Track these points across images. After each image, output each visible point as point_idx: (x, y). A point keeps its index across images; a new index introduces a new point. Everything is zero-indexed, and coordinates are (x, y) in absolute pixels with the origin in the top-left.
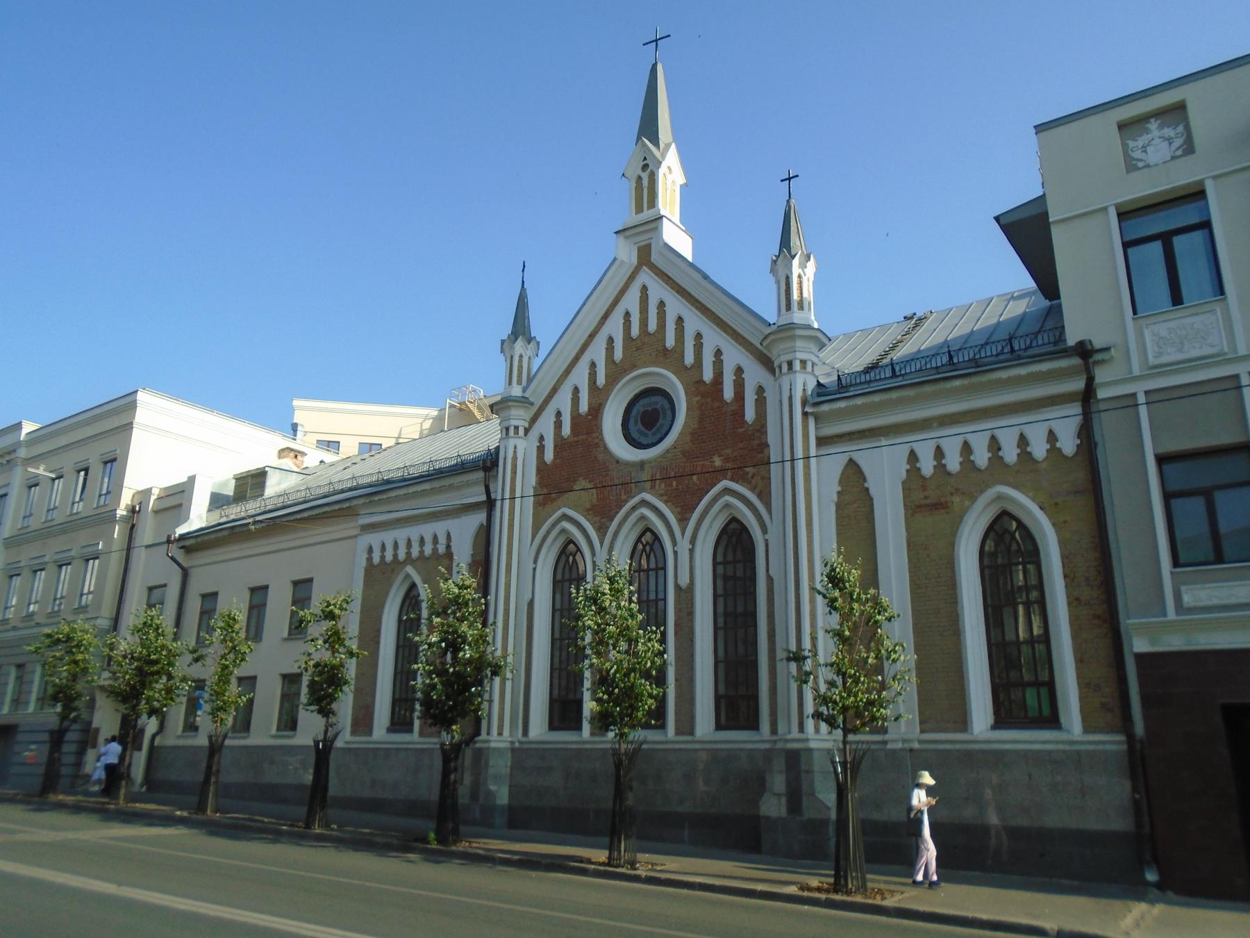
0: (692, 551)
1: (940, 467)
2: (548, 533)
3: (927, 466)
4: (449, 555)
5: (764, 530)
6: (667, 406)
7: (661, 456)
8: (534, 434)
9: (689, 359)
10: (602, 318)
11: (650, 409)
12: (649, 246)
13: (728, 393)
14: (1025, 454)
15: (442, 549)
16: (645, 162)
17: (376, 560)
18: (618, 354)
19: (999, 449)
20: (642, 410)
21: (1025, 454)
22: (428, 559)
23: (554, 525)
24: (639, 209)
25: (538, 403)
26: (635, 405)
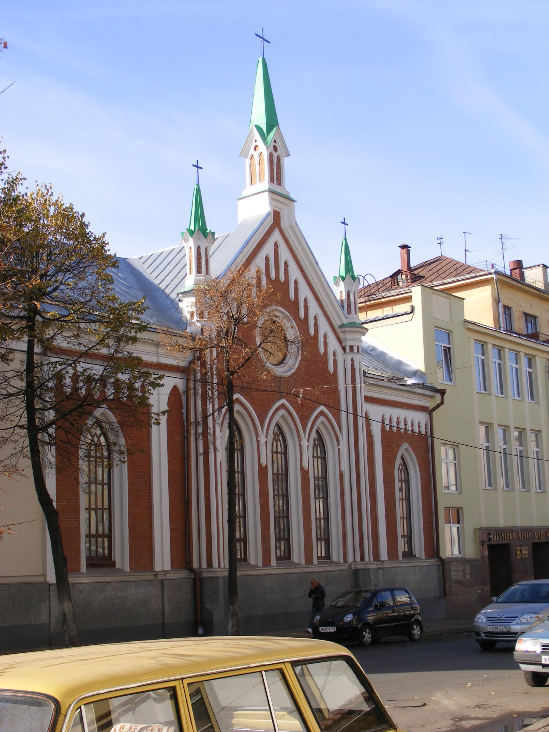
9: (302, 314)
13: (322, 349)
16: (275, 144)
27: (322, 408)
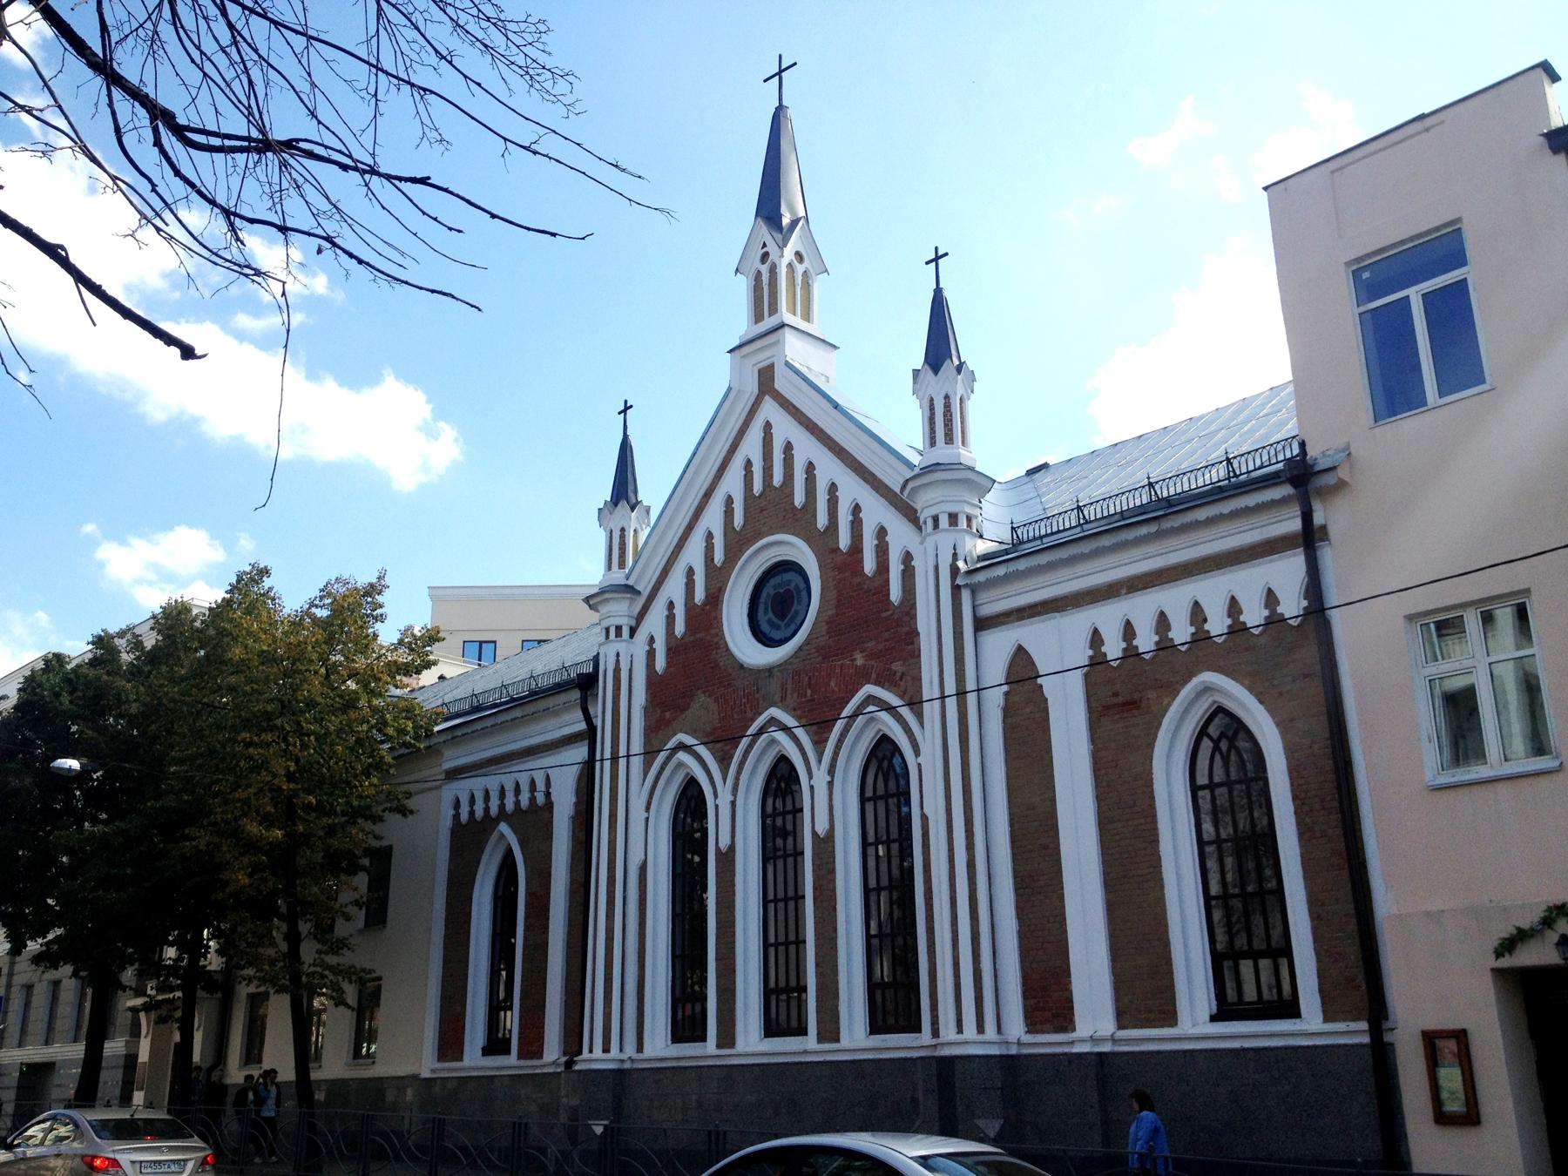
0: (831, 784)
1: (1131, 653)
2: (662, 768)
3: (1113, 648)
4: (549, 805)
5: (917, 751)
6: (802, 585)
7: (792, 657)
8: (642, 635)
9: (822, 520)
10: (718, 471)
11: (781, 591)
12: (771, 367)
13: (869, 565)
14: (1238, 630)
15: (540, 799)
16: (765, 250)
17: (464, 817)
18: (738, 520)
19: (1205, 620)
20: (772, 592)
21: (1238, 630)
22: (526, 812)
23: (668, 759)
24: (758, 317)
25: (646, 594)
26: (764, 586)
27: (869, 689)
